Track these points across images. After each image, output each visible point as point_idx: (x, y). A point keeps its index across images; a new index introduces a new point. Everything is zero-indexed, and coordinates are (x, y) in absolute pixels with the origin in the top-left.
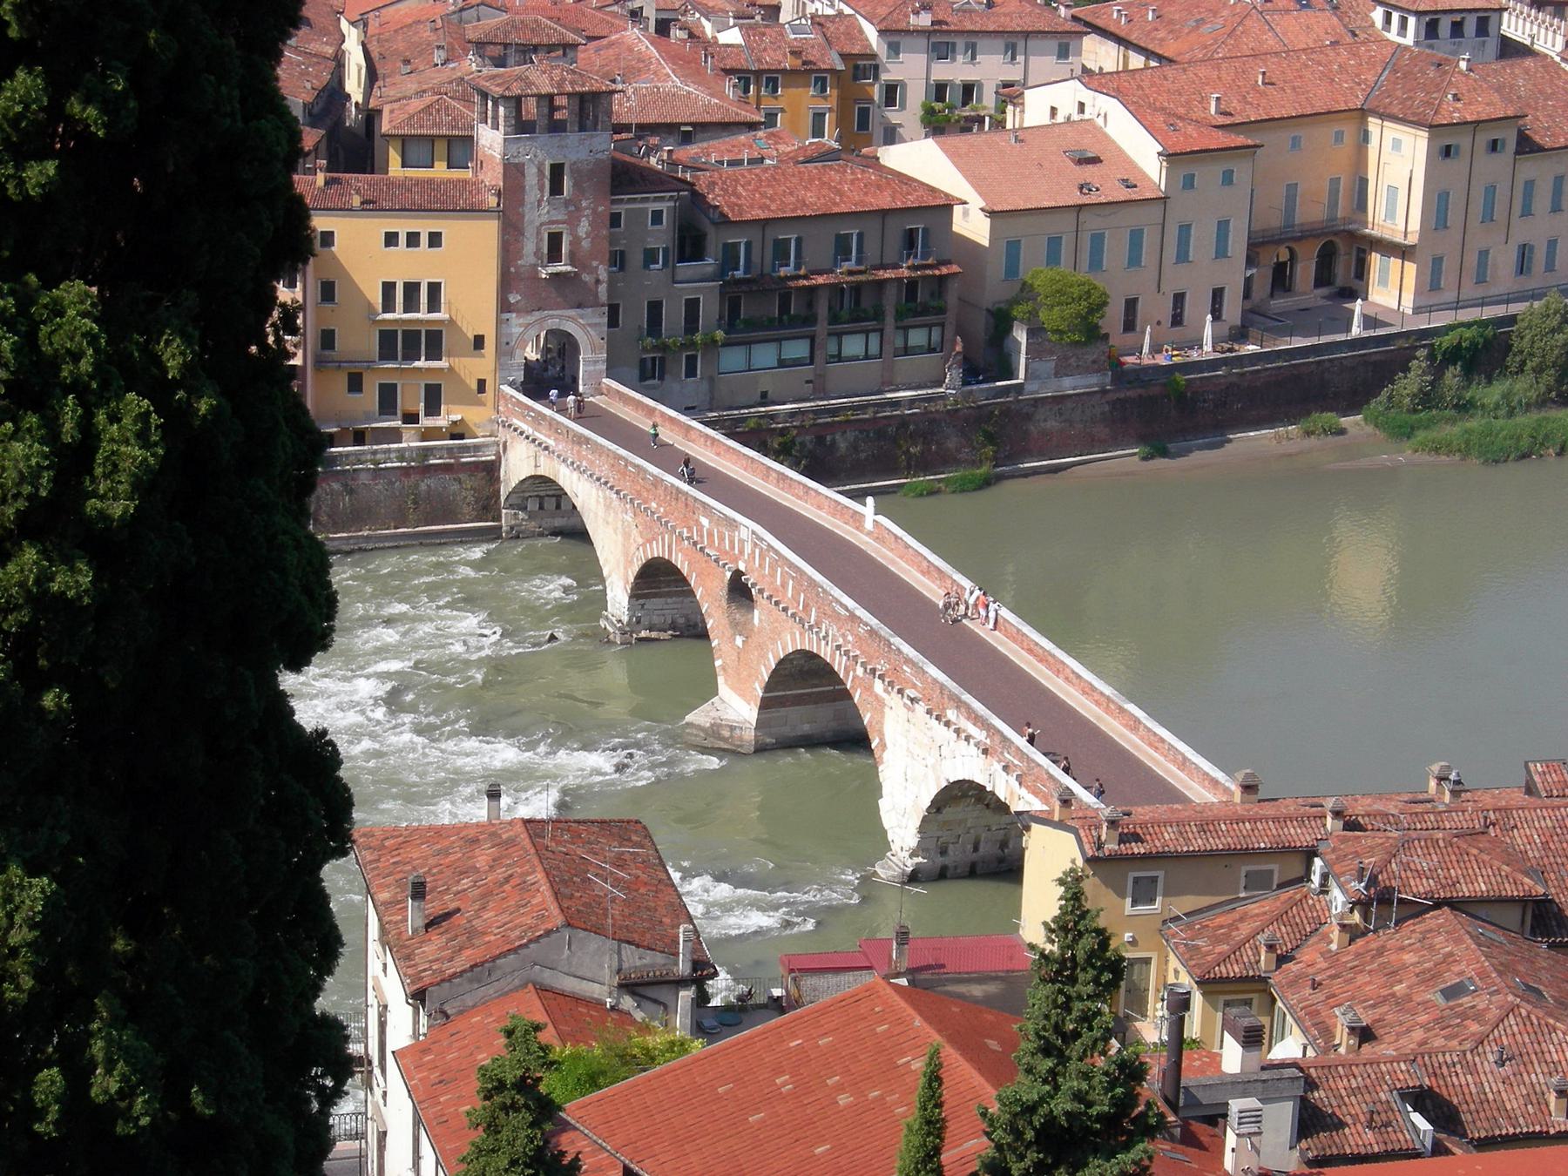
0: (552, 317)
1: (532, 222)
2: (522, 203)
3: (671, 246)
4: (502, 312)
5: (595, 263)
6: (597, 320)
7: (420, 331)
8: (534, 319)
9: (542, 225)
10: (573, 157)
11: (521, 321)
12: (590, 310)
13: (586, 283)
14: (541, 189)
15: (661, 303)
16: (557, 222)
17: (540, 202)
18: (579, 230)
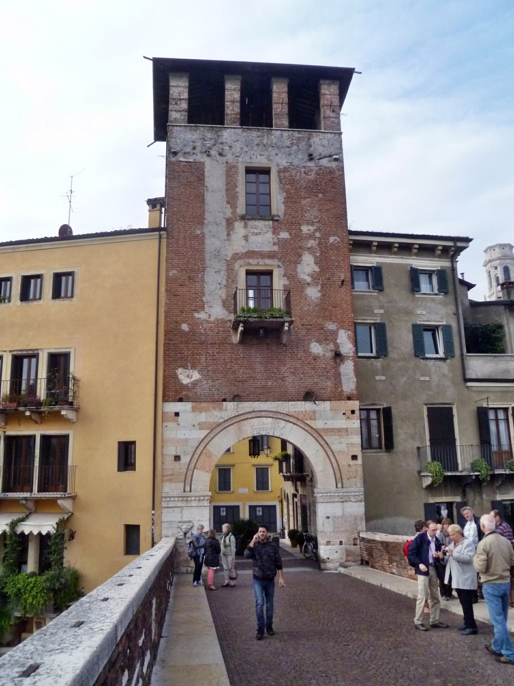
0: (259, 414)
1: (217, 254)
2: (201, 221)
3: (454, 325)
4: (166, 399)
5: (331, 326)
6: (341, 423)
7: (33, 437)
8: (226, 415)
9: (236, 257)
10: (284, 163)
11: (203, 417)
12: (327, 404)
13: (316, 358)
14: (231, 200)
15: (451, 409)
16: (262, 255)
17: (230, 223)
18: (299, 269)
